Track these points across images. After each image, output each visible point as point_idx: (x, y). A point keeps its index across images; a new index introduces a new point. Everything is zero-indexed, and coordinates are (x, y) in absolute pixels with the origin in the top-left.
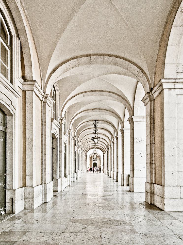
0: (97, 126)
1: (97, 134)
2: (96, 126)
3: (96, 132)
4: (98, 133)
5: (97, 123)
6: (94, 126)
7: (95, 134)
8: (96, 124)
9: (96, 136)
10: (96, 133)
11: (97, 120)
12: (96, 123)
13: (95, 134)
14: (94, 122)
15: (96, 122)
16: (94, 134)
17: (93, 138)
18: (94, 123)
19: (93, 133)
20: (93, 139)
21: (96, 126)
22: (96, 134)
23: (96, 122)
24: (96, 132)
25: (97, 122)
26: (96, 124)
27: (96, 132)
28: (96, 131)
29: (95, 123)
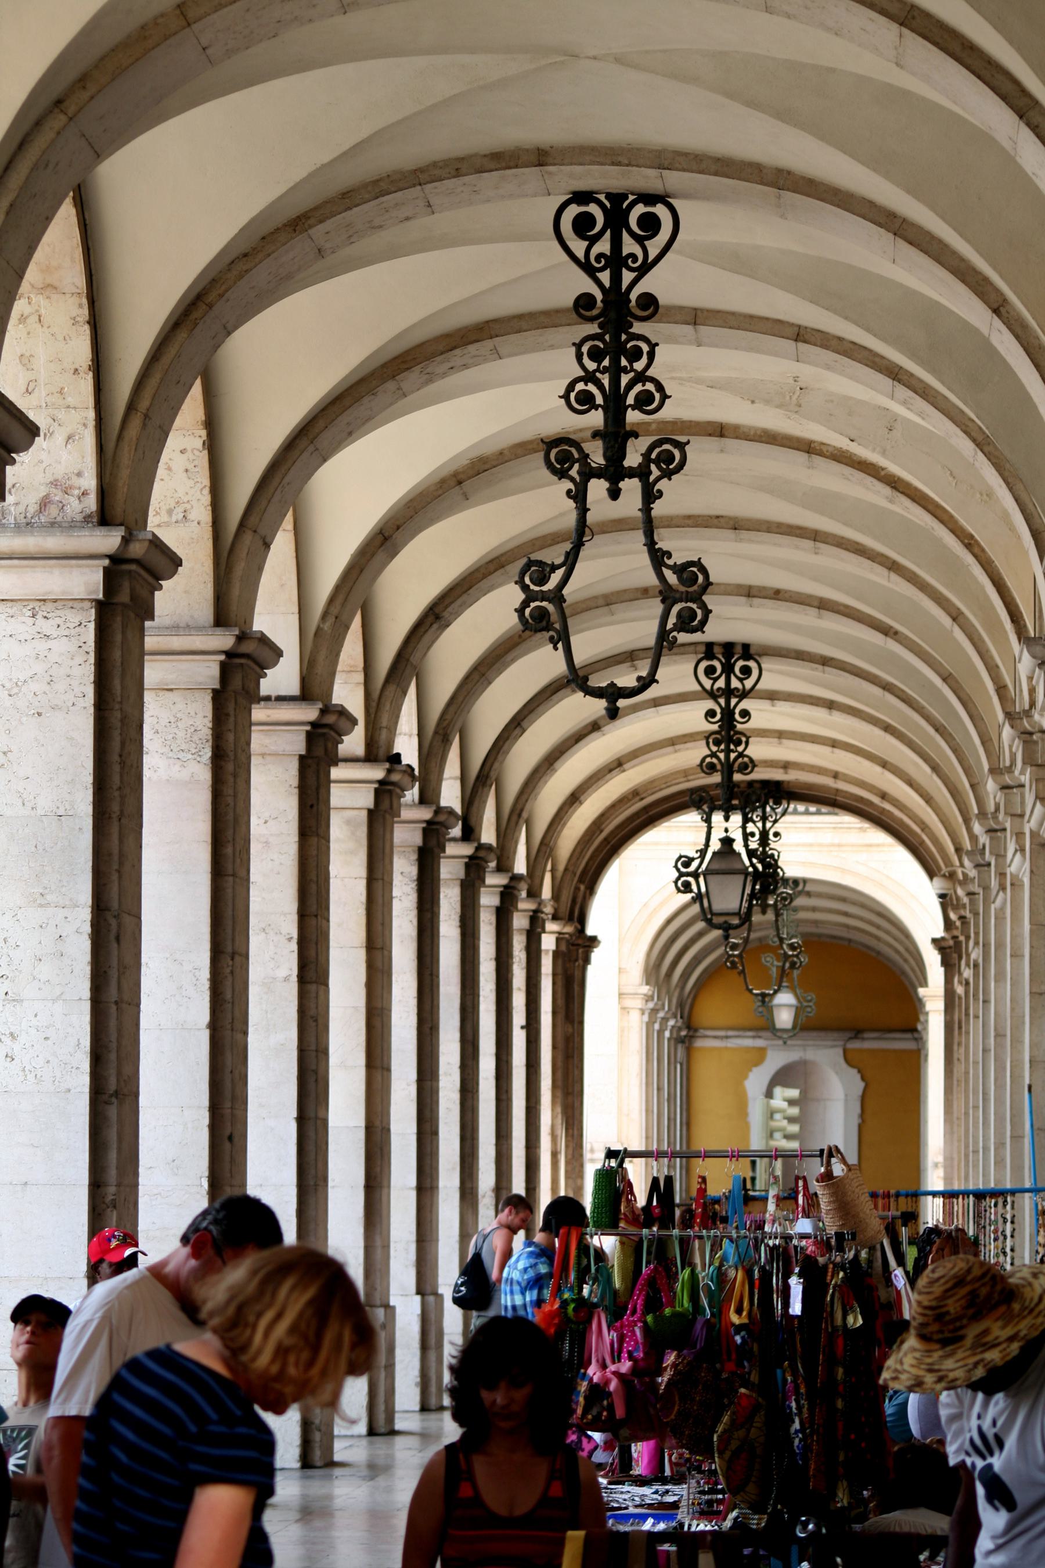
0: (745, 713)
2: (728, 715)
5: (749, 683)
6: (710, 713)
8: (728, 692)
9: (727, 842)
11: (747, 651)
12: (735, 683)
14: (710, 671)
15: (728, 669)
18: (707, 683)
20: (695, 875)
21: (728, 715)
23: (728, 669)
25: (746, 671)
26: (728, 692)
29: (721, 683)
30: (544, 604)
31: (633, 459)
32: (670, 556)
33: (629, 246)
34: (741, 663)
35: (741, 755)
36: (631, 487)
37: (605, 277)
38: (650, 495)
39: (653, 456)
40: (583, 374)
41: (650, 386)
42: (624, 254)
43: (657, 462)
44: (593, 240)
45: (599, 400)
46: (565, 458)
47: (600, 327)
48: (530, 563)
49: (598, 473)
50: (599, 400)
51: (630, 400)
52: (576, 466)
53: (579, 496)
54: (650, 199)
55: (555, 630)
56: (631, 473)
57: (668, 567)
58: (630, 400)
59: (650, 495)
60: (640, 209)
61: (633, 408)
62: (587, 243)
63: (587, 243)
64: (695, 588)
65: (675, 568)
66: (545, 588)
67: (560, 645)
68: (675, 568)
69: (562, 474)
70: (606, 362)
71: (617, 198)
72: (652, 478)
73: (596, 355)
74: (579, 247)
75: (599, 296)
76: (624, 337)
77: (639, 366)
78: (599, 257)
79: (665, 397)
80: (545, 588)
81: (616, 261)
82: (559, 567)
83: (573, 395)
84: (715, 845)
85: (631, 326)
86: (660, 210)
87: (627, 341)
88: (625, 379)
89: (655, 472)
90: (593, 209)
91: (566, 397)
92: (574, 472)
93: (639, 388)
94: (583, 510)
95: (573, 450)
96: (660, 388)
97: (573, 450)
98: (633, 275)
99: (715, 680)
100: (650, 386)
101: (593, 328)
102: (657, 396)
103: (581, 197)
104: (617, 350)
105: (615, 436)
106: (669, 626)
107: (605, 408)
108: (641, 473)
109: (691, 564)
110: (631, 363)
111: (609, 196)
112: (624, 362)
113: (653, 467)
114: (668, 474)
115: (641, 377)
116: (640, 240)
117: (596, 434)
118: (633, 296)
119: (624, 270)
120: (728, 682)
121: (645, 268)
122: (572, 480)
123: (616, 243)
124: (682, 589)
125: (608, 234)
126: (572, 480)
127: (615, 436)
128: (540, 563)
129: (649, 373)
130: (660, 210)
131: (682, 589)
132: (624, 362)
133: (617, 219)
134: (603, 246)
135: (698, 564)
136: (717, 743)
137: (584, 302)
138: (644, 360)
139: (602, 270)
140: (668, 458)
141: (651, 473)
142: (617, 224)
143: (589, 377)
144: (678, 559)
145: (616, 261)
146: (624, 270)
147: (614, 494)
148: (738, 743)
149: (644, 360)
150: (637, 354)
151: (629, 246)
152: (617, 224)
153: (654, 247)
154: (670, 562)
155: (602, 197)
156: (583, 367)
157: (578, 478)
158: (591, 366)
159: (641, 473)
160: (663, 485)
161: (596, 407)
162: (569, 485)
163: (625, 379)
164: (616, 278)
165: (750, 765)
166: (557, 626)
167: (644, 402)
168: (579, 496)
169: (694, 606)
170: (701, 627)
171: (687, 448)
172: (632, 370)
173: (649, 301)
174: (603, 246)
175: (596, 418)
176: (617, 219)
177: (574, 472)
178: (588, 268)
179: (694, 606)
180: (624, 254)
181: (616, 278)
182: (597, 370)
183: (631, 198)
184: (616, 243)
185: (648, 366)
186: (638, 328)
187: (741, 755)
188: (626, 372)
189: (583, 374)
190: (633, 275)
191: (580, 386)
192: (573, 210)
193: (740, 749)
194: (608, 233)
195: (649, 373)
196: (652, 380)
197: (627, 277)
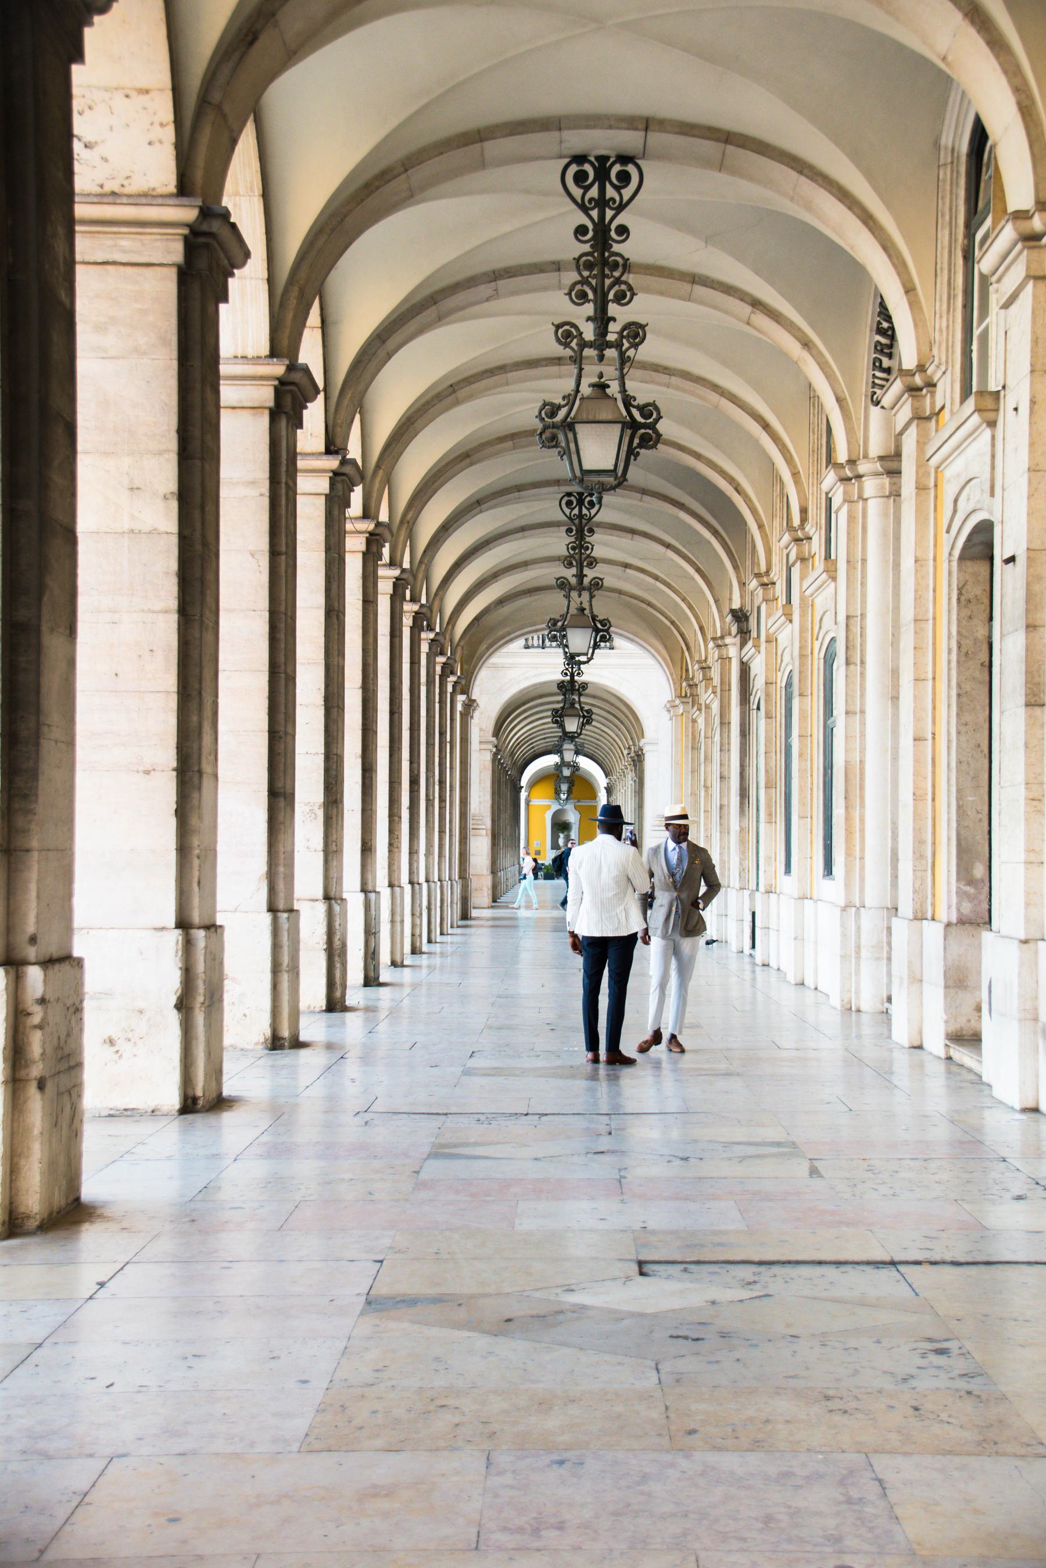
1: (592, 597)
3: (581, 576)
4: (597, 585)
5: (593, 511)
6: (569, 531)
7: (574, 594)
8: (581, 516)
10: (580, 587)
12: (585, 511)
13: (574, 594)
14: (569, 504)
16: (568, 597)
17: (555, 622)
18: (567, 511)
19: (562, 584)
22: (586, 595)
24: (581, 576)
25: (592, 504)
26: (581, 516)
27: (586, 581)
28: (586, 571)
29: (576, 511)
30: (555, 430)
31: (611, 337)
32: (635, 400)
33: (610, 192)
34: (588, 499)
35: (589, 556)
36: (611, 353)
37: (595, 213)
38: (624, 360)
39: (625, 333)
40: (579, 278)
41: (623, 287)
42: (608, 197)
43: (628, 337)
44: (587, 189)
45: (591, 296)
46: (568, 335)
47: (592, 246)
48: (545, 404)
49: (590, 344)
50: (591, 296)
51: (611, 296)
52: (575, 341)
53: (578, 360)
54: (625, 159)
55: (562, 447)
56: (609, 345)
57: (634, 407)
58: (611, 296)
59: (624, 360)
60: (617, 168)
61: (613, 301)
62: (581, 191)
63: (581, 191)
64: (651, 420)
65: (638, 407)
66: (555, 420)
67: (565, 457)
68: (638, 407)
69: (566, 345)
70: (595, 272)
71: (602, 159)
72: (624, 348)
73: (589, 266)
74: (577, 192)
75: (590, 226)
76: (607, 254)
77: (616, 274)
78: (591, 200)
79: (633, 294)
80: (555, 420)
81: (602, 203)
82: (564, 406)
83: (573, 293)
84: (573, 611)
85: (611, 246)
86: (631, 168)
87: (609, 257)
88: (608, 282)
89: (626, 345)
90: (587, 167)
91: (569, 294)
92: (574, 344)
93: (616, 288)
94: (581, 369)
95: (573, 330)
96: (630, 289)
97: (573, 330)
98: (613, 212)
99: (572, 509)
100: (623, 287)
101: (587, 248)
102: (628, 294)
103: (580, 159)
104: (605, 262)
105: (602, 320)
106: (635, 444)
107: (595, 304)
108: (618, 345)
109: (648, 405)
110: (612, 271)
111: (597, 158)
112: (607, 272)
113: (624, 341)
114: (636, 346)
115: (618, 281)
116: (618, 189)
117: (589, 319)
118: (613, 226)
119: (607, 210)
120: (580, 510)
121: (621, 208)
122: (572, 349)
123: (602, 191)
124: (643, 421)
125: (597, 184)
126: (572, 349)
127: (602, 320)
128: (552, 404)
129: (623, 278)
130: (631, 168)
131: (643, 421)
132: (607, 272)
133: (602, 175)
134: (594, 192)
135: (653, 404)
136: (573, 548)
137: (581, 230)
138: (620, 269)
139: (592, 209)
140: (636, 332)
141: (623, 345)
142: (602, 179)
143: (584, 281)
144: (641, 401)
145: (602, 203)
146: (607, 210)
147: (601, 358)
148: (588, 548)
149: (620, 269)
150: (616, 265)
151: (610, 192)
152: (602, 179)
153: (627, 193)
154: (635, 403)
155: (592, 159)
156: (580, 274)
157: (576, 348)
158: (586, 274)
159: (618, 345)
160: (631, 353)
161: (589, 301)
162: (568, 352)
163: (608, 282)
164: (602, 216)
165: (593, 562)
166: (563, 444)
167: (620, 298)
168: (578, 360)
169: (651, 432)
170: (654, 446)
171: (646, 328)
172: (612, 276)
173: (623, 230)
174: (594, 192)
175: (589, 309)
176: (602, 175)
177: (574, 344)
178: (584, 208)
179: (651, 432)
180: (608, 197)
181: (602, 216)
182: (589, 276)
183: (612, 160)
184: (602, 191)
185: (622, 274)
186: (616, 248)
187: (589, 556)
188: (609, 278)
189: (579, 278)
190: (613, 212)
191: (578, 287)
192: (573, 169)
193: (588, 552)
194: (597, 184)
195: (623, 278)
196: (626, 283)
197: (609, 213)
